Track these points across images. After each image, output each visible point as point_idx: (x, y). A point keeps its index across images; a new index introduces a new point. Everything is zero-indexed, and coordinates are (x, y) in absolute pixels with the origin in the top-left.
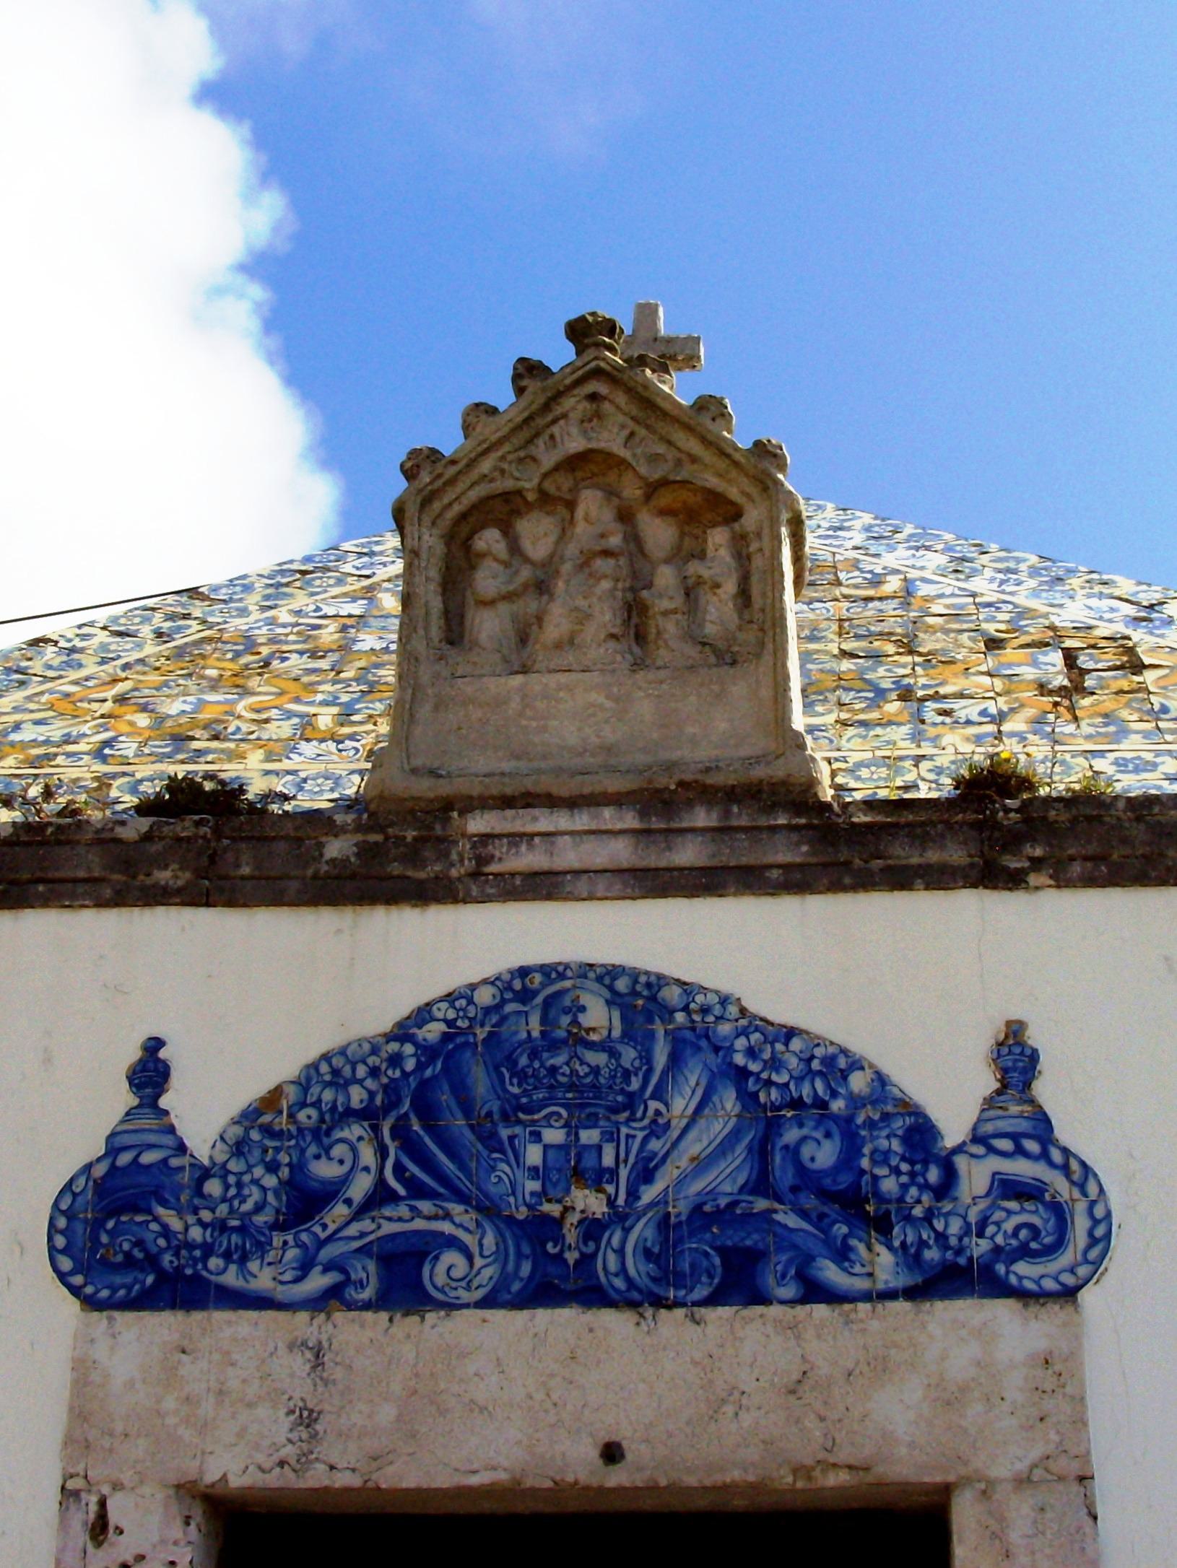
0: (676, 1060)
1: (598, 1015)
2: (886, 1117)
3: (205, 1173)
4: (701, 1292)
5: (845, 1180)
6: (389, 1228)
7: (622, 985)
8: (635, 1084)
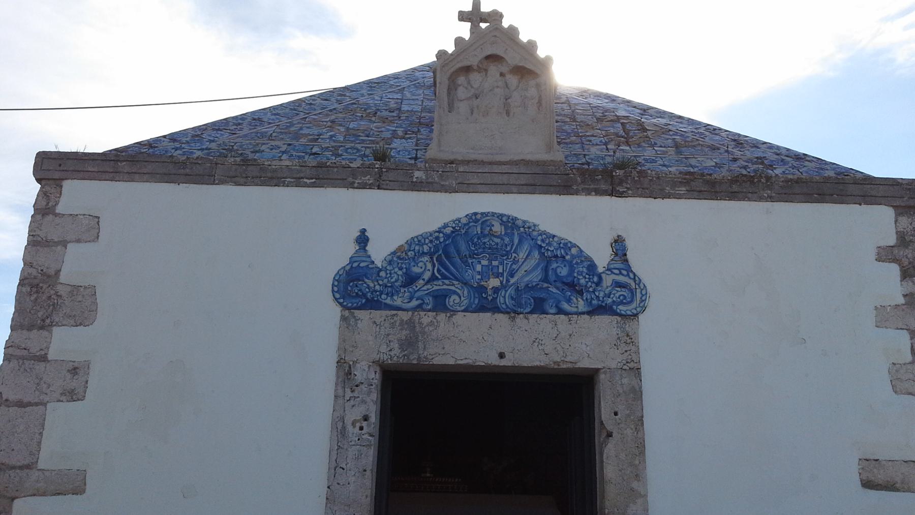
0: (520, 241)
1: (497, 228)
2: (582, 261)
3: (381, 270)
4: (528, 310)
5: (570, 279)
6: (436, 288)
8: (508, 248)
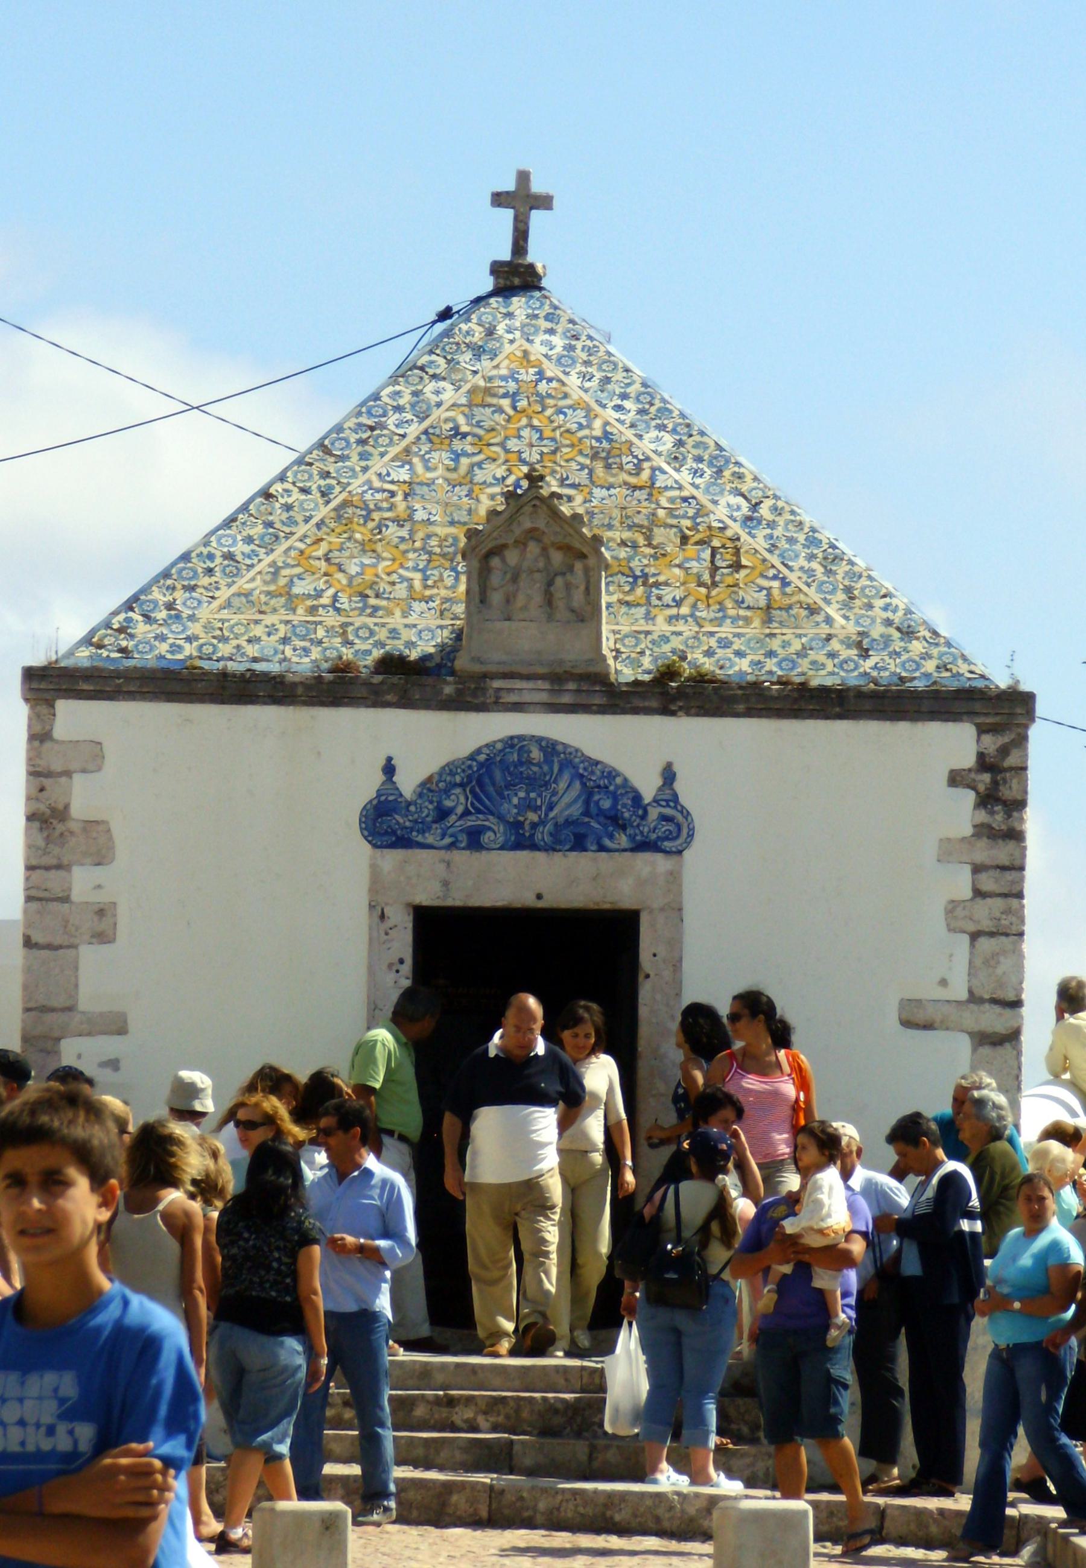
0: (560, 770)
1: (536, 754)
2: (627, 792)
3: (409, 804)
4: (567, 847)
5: (613, 813)
6: (470, 823)
7: (544, 744)
8: (547, 778)
